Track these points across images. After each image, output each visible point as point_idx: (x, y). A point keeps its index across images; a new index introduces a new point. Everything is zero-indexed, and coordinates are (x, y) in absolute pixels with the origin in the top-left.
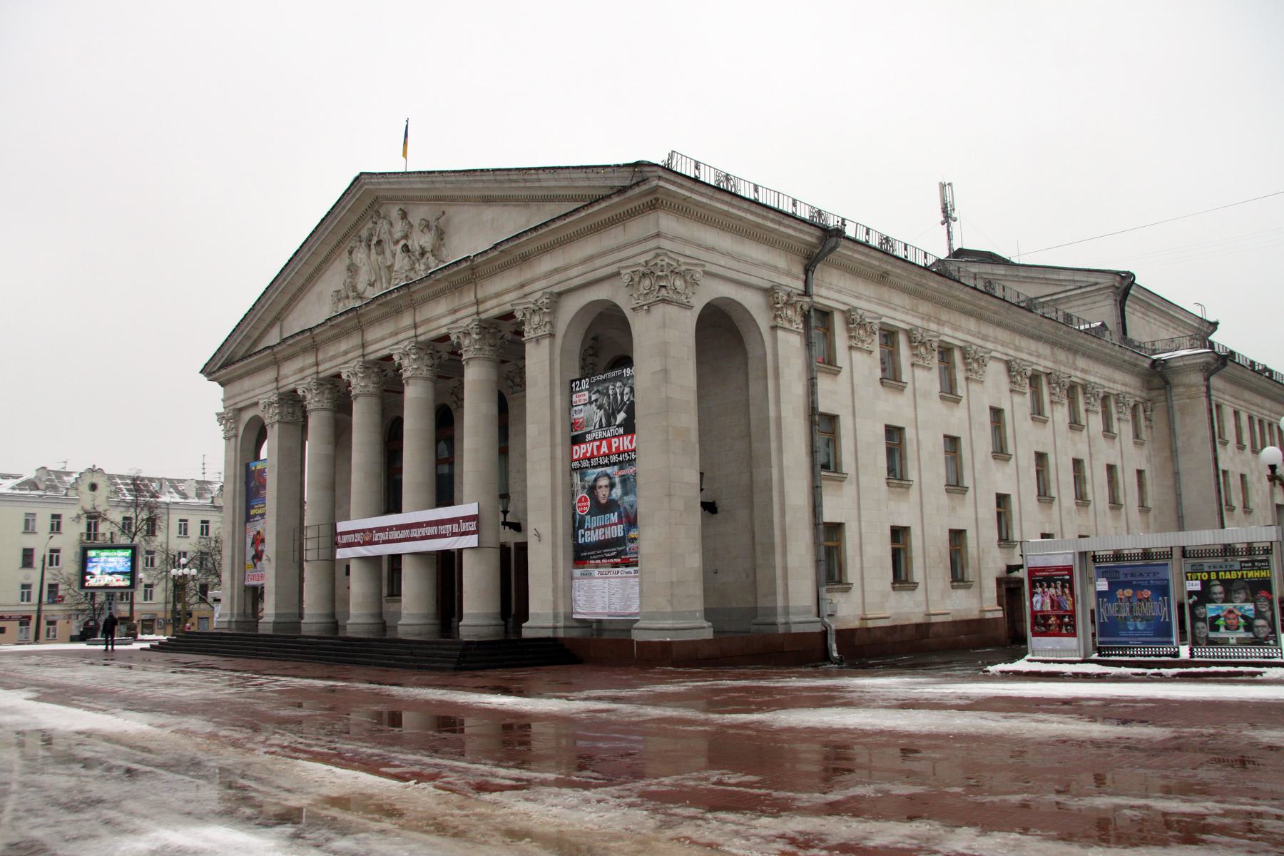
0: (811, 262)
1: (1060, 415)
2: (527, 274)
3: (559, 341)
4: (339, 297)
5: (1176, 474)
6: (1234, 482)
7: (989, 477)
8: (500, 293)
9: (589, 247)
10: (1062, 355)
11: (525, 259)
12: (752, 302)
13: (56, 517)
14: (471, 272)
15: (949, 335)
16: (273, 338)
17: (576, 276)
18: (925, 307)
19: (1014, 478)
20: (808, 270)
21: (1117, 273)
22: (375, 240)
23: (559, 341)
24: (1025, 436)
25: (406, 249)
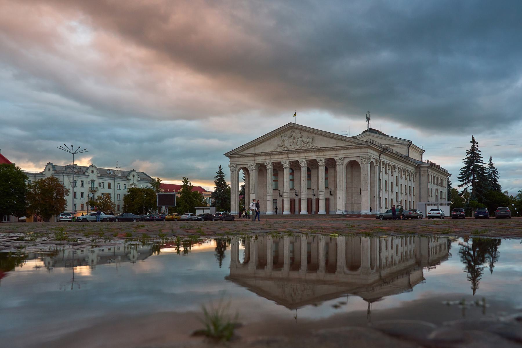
0: (381, 153)
1: (404, 177)
2: (338, 153)
3: (344, 165)
4: (279, 146)
5: (420, 188)
6: (430, 190)
7: (397, 189)
8: (330, 155)
9: (353, 151)
10: (405, 165)
11: (337, 150)
12: (374, 161)
13: (82, 181)
14: (324, 150)
15: (394, 164)
16: (251, 151)
17: (349, 155)
18: (390, 159)
19: (397, 189)
20: (380, 155)
21: (408, 141)
22: (292, 137)
23: (344, 165)
24: (400, 181)
25: (302, 141)
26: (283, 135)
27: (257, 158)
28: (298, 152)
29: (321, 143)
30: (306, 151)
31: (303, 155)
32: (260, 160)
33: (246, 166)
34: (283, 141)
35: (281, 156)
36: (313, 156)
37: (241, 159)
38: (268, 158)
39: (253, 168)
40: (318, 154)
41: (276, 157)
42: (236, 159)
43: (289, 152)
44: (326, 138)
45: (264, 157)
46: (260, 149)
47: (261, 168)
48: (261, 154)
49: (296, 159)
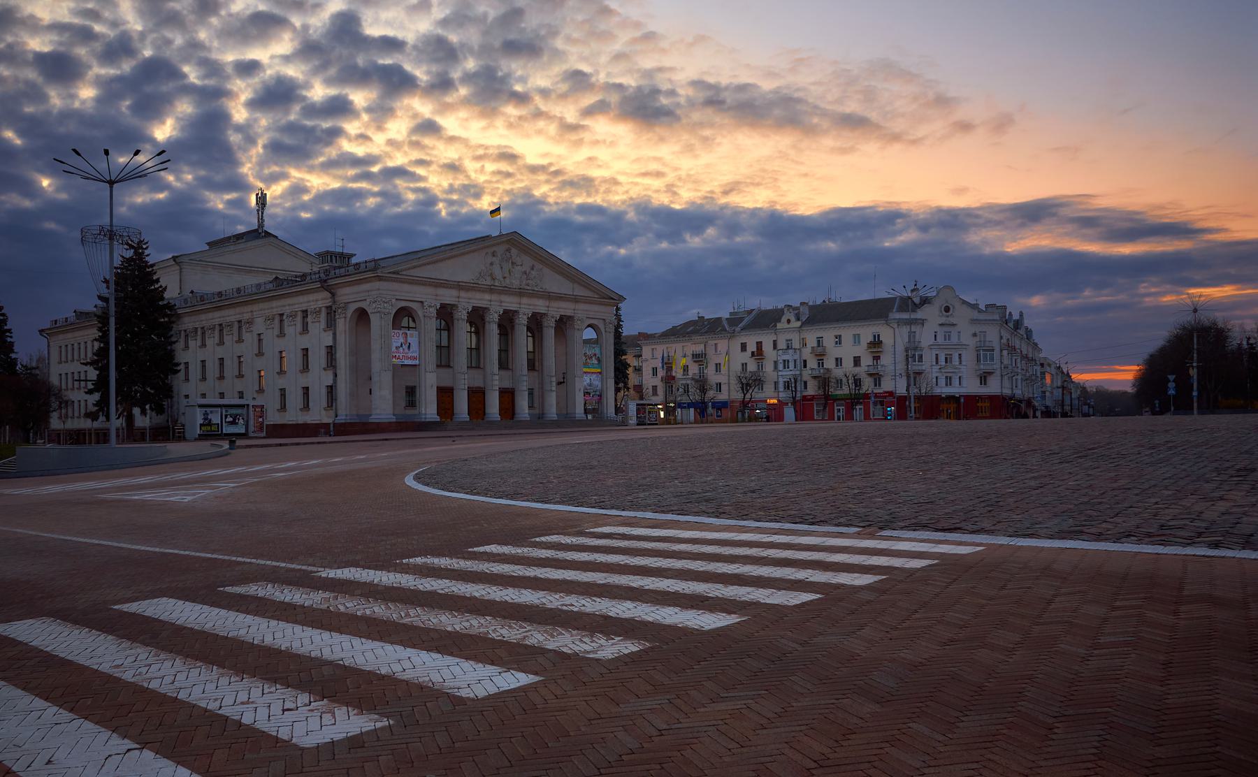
8: (566, 308)
9: (596, 308)
26: (490, 250)
27: (441, 291)
28: (521, 293)
29: (555, 284)
30: (534, 295)
31: (525, 300)
32: (448, 296)
33: (414, 306)
34: (492, 264)
35: (487, 297)
36: (540, 306)
37: (406, 287)
38: (463, 294)
39: (433, 312)
40: (547, 303)
41: (478, 295)
42: (395, 286)
43: (506, 291)
44: (558, 277)
45: (454, 292)
46: (446, 271)
47: (446, 314)
48: (460, 286)
49: (513, 307)
